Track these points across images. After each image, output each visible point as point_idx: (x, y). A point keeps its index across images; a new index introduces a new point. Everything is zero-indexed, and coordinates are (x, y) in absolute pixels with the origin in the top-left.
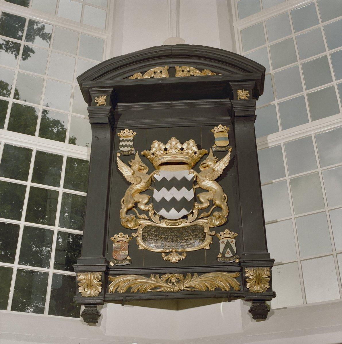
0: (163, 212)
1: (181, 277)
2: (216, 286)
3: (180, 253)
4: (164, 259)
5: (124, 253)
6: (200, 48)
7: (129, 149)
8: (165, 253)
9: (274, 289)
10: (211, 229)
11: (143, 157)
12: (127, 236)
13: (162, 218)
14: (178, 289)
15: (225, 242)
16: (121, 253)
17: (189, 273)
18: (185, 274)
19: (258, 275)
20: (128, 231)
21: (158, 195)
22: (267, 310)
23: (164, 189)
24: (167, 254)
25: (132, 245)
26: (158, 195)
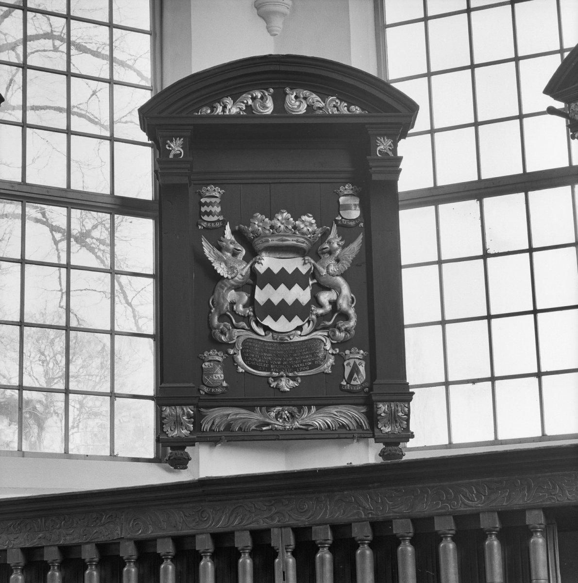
0: (268, 321)
1: (295, 409)
2: (339, 424)
3: (294, 379)
4: (272, 386)
5: (219, 375)
7: (215, 218)
8: (273, 377)
9: (412, 429)
10: (333, 346)
11: (239, 235)
12: (221, 354)
13: (266, 329)
14: (291, 427)
16: (214, 378)
17: (305, 406)
18: (300, 408)
19: (393, 410)
21: (261, 296)
22: (403, 454)
23: (269, 287)
25: (230, 364)
26: (261, 296)
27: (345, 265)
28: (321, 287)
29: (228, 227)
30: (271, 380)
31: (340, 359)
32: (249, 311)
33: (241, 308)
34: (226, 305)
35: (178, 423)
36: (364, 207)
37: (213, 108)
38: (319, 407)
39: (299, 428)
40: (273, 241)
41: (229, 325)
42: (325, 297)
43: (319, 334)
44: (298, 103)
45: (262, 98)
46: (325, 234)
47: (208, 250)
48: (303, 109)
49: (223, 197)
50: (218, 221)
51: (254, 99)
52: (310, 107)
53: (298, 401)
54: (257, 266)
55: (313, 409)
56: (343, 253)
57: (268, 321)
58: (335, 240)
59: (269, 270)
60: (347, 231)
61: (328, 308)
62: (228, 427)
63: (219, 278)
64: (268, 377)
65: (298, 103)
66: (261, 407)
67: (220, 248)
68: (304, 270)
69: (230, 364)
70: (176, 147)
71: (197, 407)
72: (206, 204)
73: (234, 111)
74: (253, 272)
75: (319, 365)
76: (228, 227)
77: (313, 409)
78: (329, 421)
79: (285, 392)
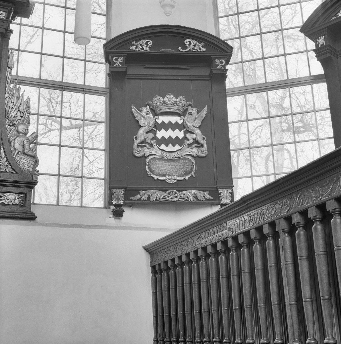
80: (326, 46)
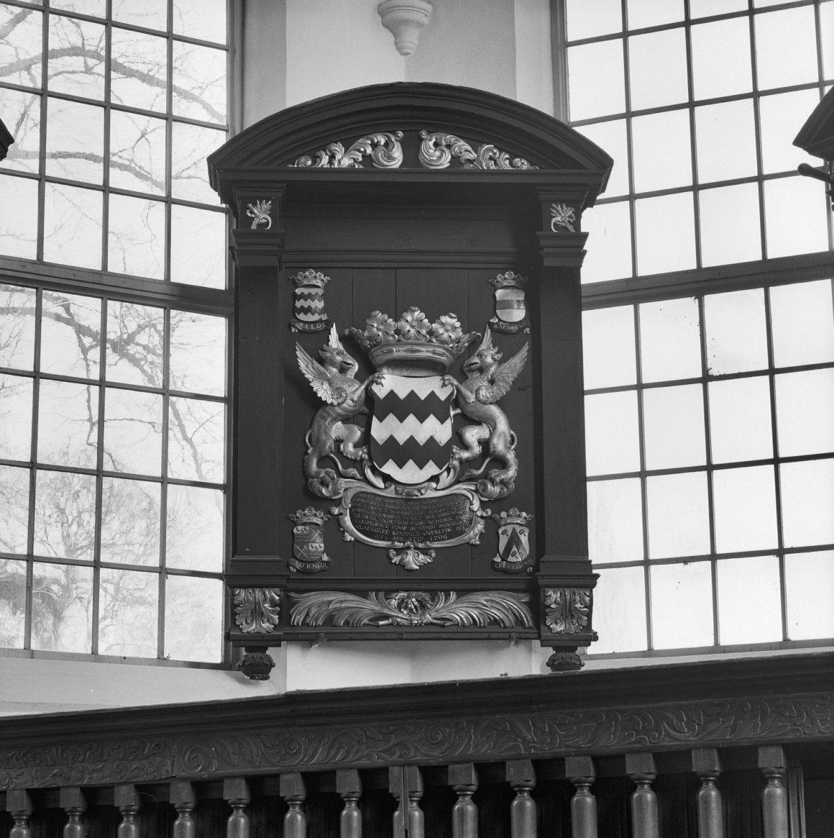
0: (390, 468)
1: (426, 596)
2: (489, 618)
3: (425, 551)
4: (393, 561)
5: (318, 545)
6: (509, 586)
7: (316, 317)
8: (395, 549)
9: (594, 628)
10: (483, 505)
11: (350, 342)
12: (320, 514)
13: (387, 479)
14: (420, 621)
15: (509, 533)
16: (310, 548)
17: (441, 591)
18: (434, 594)
19: (568, 604)
20: (324, 503)
21: (381, 430)
22: (581, 664)
23: (391, 418)
24: (399, 551)
25: (333, 529)
26: (381, 430)
27: (503, 389)
28: (467, 419)
29: (334, 331)
30: (392, 552)
31: (493, 525)
32: (362, 453)
33: (350, 448)
34: (330, 444)
35: (258, 614)
36: (532, 305)
37: (316, 159)
38: (461, 593)
39: (432, 624)
40: (399, 352)
41: (333, 472)
42: (473, 435)
43: (462, 488)
44: (438, 153)
45: (386, 145)
46: (475, 343)
47: (305, 364)
48: (445, 162)
49: (327, 287)
50: (320, 321)
51: (375, 146)
52: (455, 160)
53: (430, 584)
54: (375, 388)
55: (453, 596)
56: (499, 372)
57: (390, 468)
58: (488, 353)
59: (392, 394)
60: (506, 339)
61: (477, 450)
62: (330, 620)
63: (320, 404)
64: (387, 549)
65: (438, 153)
66: (377, 591)
67: (322, 361)
68: (443, 395)
69: (333, 529)
70: (261, 214)
71: (285, 590)
72: (303, 296)
73: (346, 162)
74: (369, 397)
75: (462, 533)
76: (334, 331)
77: (453, 596)
78: (475, 613)
79: (413, 570)
80: (270, 234)
